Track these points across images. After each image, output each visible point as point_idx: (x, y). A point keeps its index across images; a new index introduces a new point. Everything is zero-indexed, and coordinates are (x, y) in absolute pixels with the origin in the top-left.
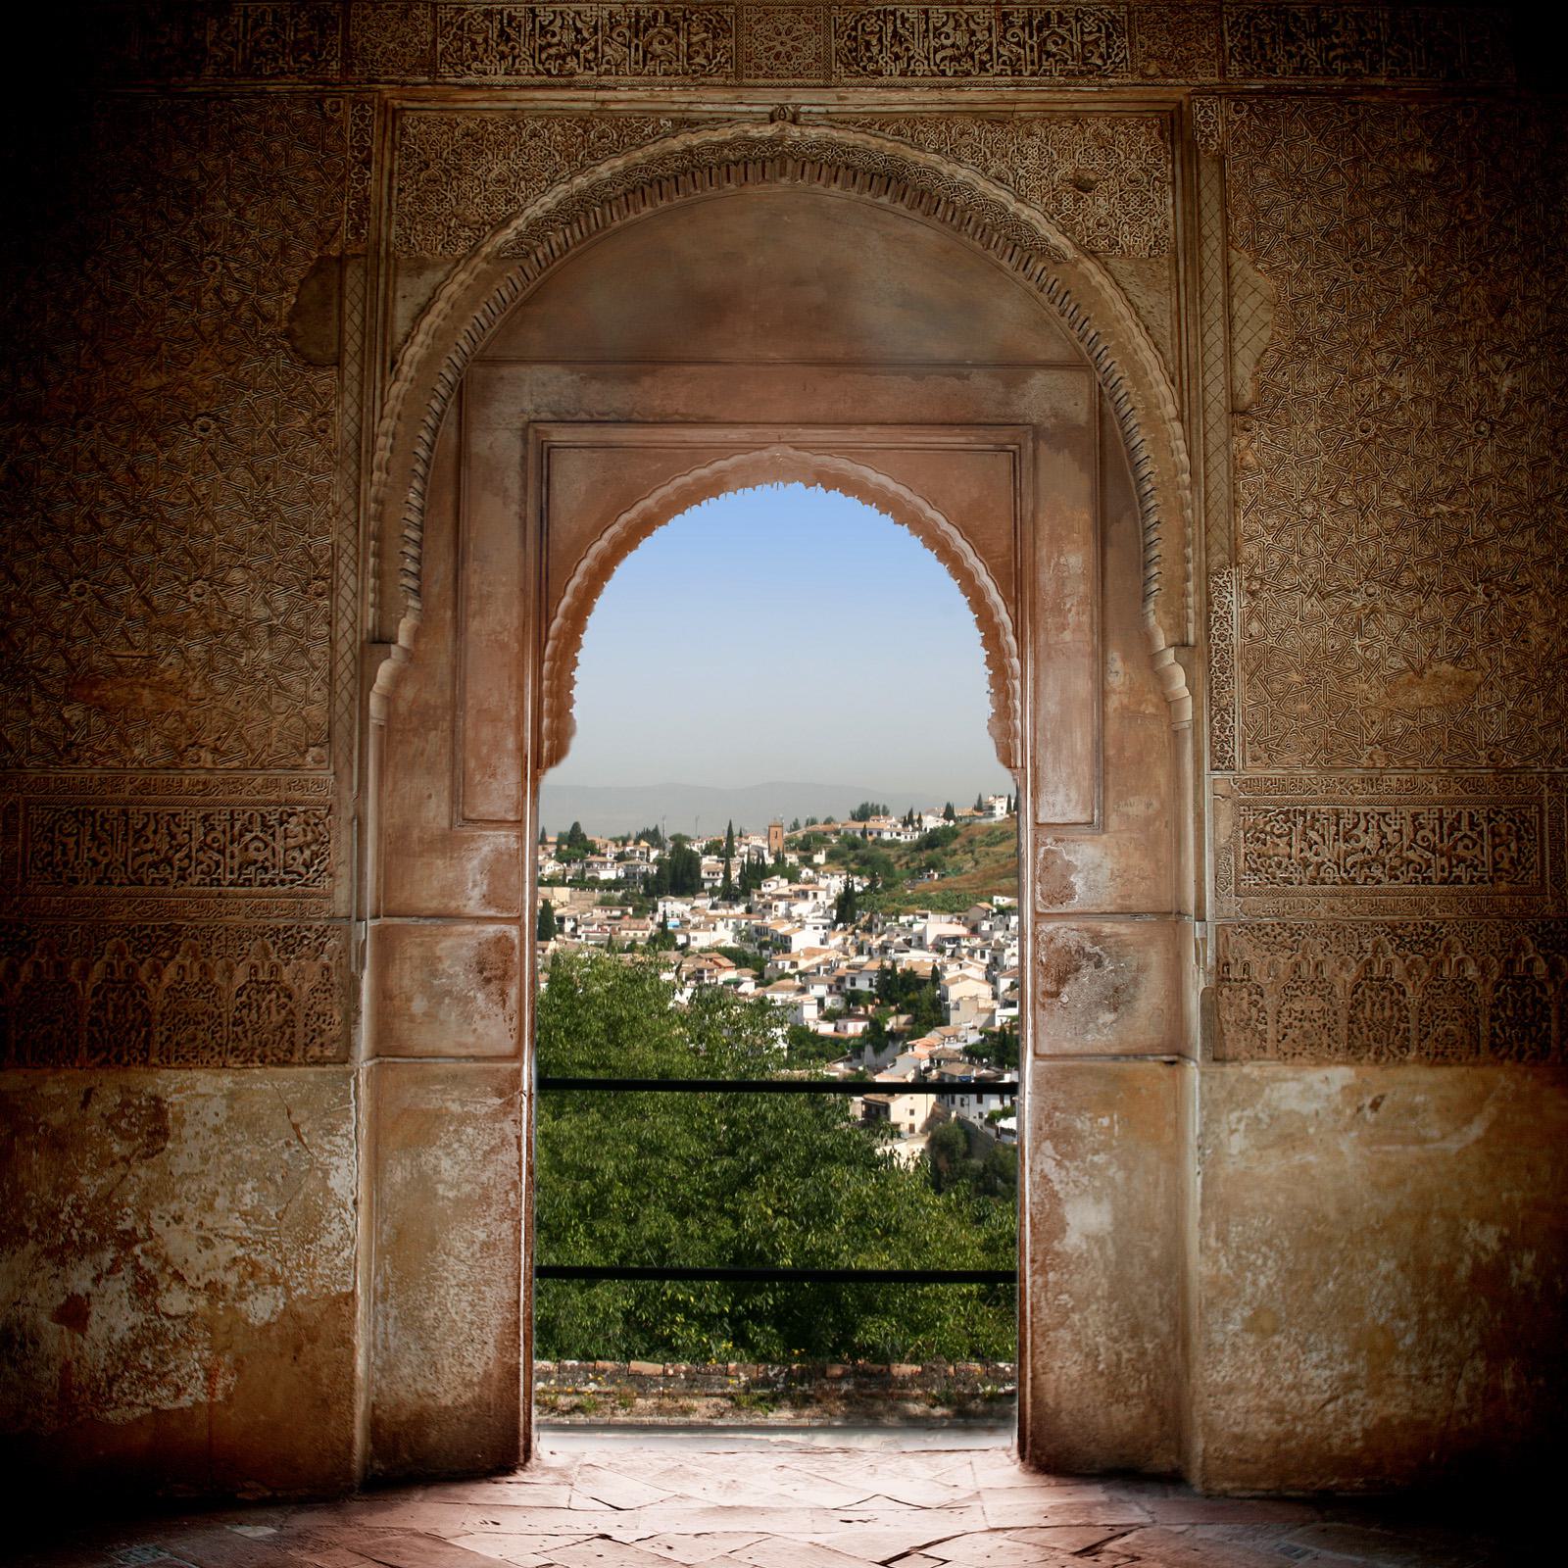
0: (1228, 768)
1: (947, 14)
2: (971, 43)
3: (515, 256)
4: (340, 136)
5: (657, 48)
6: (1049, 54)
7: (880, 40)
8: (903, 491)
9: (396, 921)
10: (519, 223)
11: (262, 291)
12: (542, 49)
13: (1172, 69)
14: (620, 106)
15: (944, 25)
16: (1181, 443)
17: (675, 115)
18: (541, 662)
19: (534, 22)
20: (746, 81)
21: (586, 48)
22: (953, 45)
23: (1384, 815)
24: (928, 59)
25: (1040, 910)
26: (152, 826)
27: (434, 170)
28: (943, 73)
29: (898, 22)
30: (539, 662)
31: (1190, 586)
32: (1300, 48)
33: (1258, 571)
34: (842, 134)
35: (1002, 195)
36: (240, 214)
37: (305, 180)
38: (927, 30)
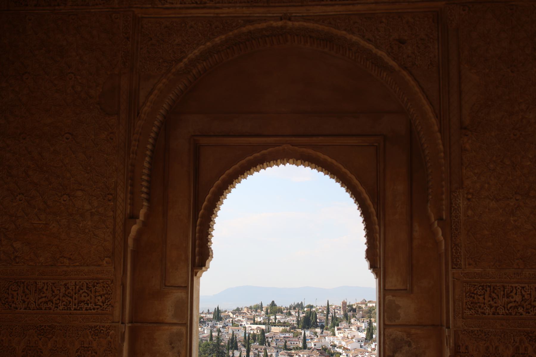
0: (459, 268)
8: (334, 161)
9: (139, 324)
10: (185, 60)
14: (224, 15)
16: (440, 141)
18: (196, 227)
23: (523, 288)
25: (387, 323)
26: (45, 287)
30: (195, 226)
31: (444, 197)
33: (471, 191)
35: (371, 46)
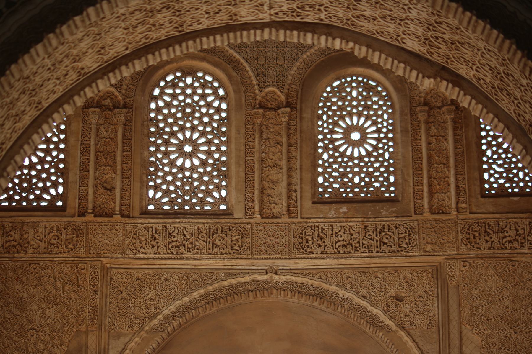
1: (341, 226)
2: (351, 239)
3: (159, 331)
4: (85, 280)
5: (218, 243)
6: (384, 243)
7: (312, 238)
10: (160, 317)
11: (53, 345)
12: (170, 243)
13: (436, 248)
15: (339, 231)
17: (225, 271)
19: (166, 232)
20: (255, 256)
21: (188, 242)
22: (343, 240)
24: (332, 246)
27: (124, 295)
28: (339, 252)
29: (320, 230)
32: (491, 238)
34: (297, 278)
35: (365, 304)
36: (43, 312)
37: (70, 298)
38: (332, 234)
